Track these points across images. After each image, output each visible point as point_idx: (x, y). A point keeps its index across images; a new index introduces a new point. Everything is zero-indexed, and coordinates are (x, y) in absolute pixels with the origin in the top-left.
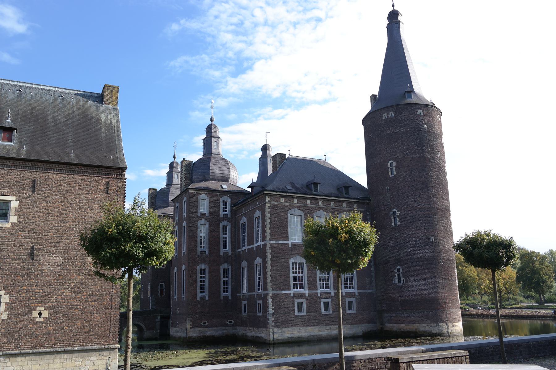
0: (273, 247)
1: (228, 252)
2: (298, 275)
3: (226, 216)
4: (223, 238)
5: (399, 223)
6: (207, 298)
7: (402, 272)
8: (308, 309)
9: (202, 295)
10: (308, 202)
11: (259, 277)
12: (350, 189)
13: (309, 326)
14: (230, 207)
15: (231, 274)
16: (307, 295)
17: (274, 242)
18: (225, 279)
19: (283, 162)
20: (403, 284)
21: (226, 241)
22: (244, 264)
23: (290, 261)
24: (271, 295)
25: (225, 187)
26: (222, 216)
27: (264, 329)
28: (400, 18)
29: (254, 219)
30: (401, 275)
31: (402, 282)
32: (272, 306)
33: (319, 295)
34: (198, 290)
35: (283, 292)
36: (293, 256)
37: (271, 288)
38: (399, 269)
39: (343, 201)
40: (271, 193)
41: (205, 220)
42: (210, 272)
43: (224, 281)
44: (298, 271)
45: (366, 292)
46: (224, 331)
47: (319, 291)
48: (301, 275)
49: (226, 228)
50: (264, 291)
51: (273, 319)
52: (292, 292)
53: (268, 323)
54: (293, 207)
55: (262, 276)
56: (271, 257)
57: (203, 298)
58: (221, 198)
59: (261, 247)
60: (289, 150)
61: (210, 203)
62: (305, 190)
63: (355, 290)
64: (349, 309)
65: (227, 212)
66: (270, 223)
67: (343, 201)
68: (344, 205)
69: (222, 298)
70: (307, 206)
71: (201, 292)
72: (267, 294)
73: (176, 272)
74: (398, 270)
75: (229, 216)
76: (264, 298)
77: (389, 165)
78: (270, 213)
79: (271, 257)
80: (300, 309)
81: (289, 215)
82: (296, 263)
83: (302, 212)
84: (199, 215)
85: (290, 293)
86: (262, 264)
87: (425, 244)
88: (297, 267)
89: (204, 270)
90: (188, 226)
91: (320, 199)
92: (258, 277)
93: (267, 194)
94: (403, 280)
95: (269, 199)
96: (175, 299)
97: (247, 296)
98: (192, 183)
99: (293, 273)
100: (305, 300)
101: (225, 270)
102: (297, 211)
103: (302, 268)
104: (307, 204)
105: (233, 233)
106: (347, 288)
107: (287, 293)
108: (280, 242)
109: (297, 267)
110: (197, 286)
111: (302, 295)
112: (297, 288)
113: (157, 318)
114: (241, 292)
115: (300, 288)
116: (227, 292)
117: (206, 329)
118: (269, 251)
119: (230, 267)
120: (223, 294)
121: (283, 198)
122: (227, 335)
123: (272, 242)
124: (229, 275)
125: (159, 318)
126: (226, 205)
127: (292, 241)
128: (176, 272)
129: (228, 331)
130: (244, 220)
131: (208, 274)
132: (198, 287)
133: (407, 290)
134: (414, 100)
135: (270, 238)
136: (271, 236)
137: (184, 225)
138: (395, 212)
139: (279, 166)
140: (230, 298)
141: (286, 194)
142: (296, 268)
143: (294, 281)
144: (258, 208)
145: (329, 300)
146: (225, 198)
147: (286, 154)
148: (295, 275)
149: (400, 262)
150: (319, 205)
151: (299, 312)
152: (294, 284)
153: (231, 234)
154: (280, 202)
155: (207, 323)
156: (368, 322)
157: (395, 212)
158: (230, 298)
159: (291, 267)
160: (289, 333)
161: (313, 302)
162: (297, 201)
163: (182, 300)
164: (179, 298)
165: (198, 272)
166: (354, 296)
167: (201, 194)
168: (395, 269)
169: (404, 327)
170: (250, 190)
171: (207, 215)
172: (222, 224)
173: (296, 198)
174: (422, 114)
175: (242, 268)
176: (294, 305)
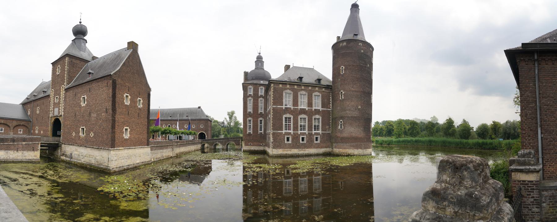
0: (274, 109)
1: (262, 113)
5: (343, 98)
6: (252, 133)
8: (292, 140)
10: (296, 87)
13: (293, 149)
16: (292, 134)
17: (275, 106)
18: (261, 125)
20: (343, 129)
24: (272, 133)
25: (262, 82)
26: (259, 95)
31: (342, 128)
33: (299, 134)
34: (248, 129)
36: (285, 113)
39: (316, 87)
41: (251, 97)
42: (253, 121)
44: (288, 121)
45: (326, 133)
47: (299, 132)
48: (289, 123)
52: (284, 131)
54: (287, 89)
57: (250, 133)
61: (253, 90)
63: (320, 132)
64: (316, 141)
66: (273, 97)
68: (317, 89)
69: (259, 133)
71: (249, 130)
74: (341, 122)
75: (263, 96)
78: (273, 92)
84: (248, 95)
87: (356, 109)
88: (288, 119)
89: (251, 120)
93: (272, 83)
100: (291, 136)
101: (261, 121)
102: (288, 91)
108: (278, 107)
109: (288, 119)
110: (247, 127)
111: (290, 134)
112: (287, 130)
116: (262, 131)
117: (251, 147)
120: (259, 132)
122: (261, 150)
123: (273, 106)
124: (263, 123)
129: (261, 148)
136: (273, 104)
138: (342, 92)
140: (263, 133)
142: (287, 120)
143: (285, 126)
145: (305, 136)
146: (262, 87)
148: (286, 123)
149: (342, 118)
156: (326, 147)
157: (342, 92)
158: (263, 133)
159: (284, 119)
160: (280, 152)
161: (296, 137)
166: (319, 135)
167: (249, 86)
171: (252, 95)
172: (260, 99)
176: (284, 138)
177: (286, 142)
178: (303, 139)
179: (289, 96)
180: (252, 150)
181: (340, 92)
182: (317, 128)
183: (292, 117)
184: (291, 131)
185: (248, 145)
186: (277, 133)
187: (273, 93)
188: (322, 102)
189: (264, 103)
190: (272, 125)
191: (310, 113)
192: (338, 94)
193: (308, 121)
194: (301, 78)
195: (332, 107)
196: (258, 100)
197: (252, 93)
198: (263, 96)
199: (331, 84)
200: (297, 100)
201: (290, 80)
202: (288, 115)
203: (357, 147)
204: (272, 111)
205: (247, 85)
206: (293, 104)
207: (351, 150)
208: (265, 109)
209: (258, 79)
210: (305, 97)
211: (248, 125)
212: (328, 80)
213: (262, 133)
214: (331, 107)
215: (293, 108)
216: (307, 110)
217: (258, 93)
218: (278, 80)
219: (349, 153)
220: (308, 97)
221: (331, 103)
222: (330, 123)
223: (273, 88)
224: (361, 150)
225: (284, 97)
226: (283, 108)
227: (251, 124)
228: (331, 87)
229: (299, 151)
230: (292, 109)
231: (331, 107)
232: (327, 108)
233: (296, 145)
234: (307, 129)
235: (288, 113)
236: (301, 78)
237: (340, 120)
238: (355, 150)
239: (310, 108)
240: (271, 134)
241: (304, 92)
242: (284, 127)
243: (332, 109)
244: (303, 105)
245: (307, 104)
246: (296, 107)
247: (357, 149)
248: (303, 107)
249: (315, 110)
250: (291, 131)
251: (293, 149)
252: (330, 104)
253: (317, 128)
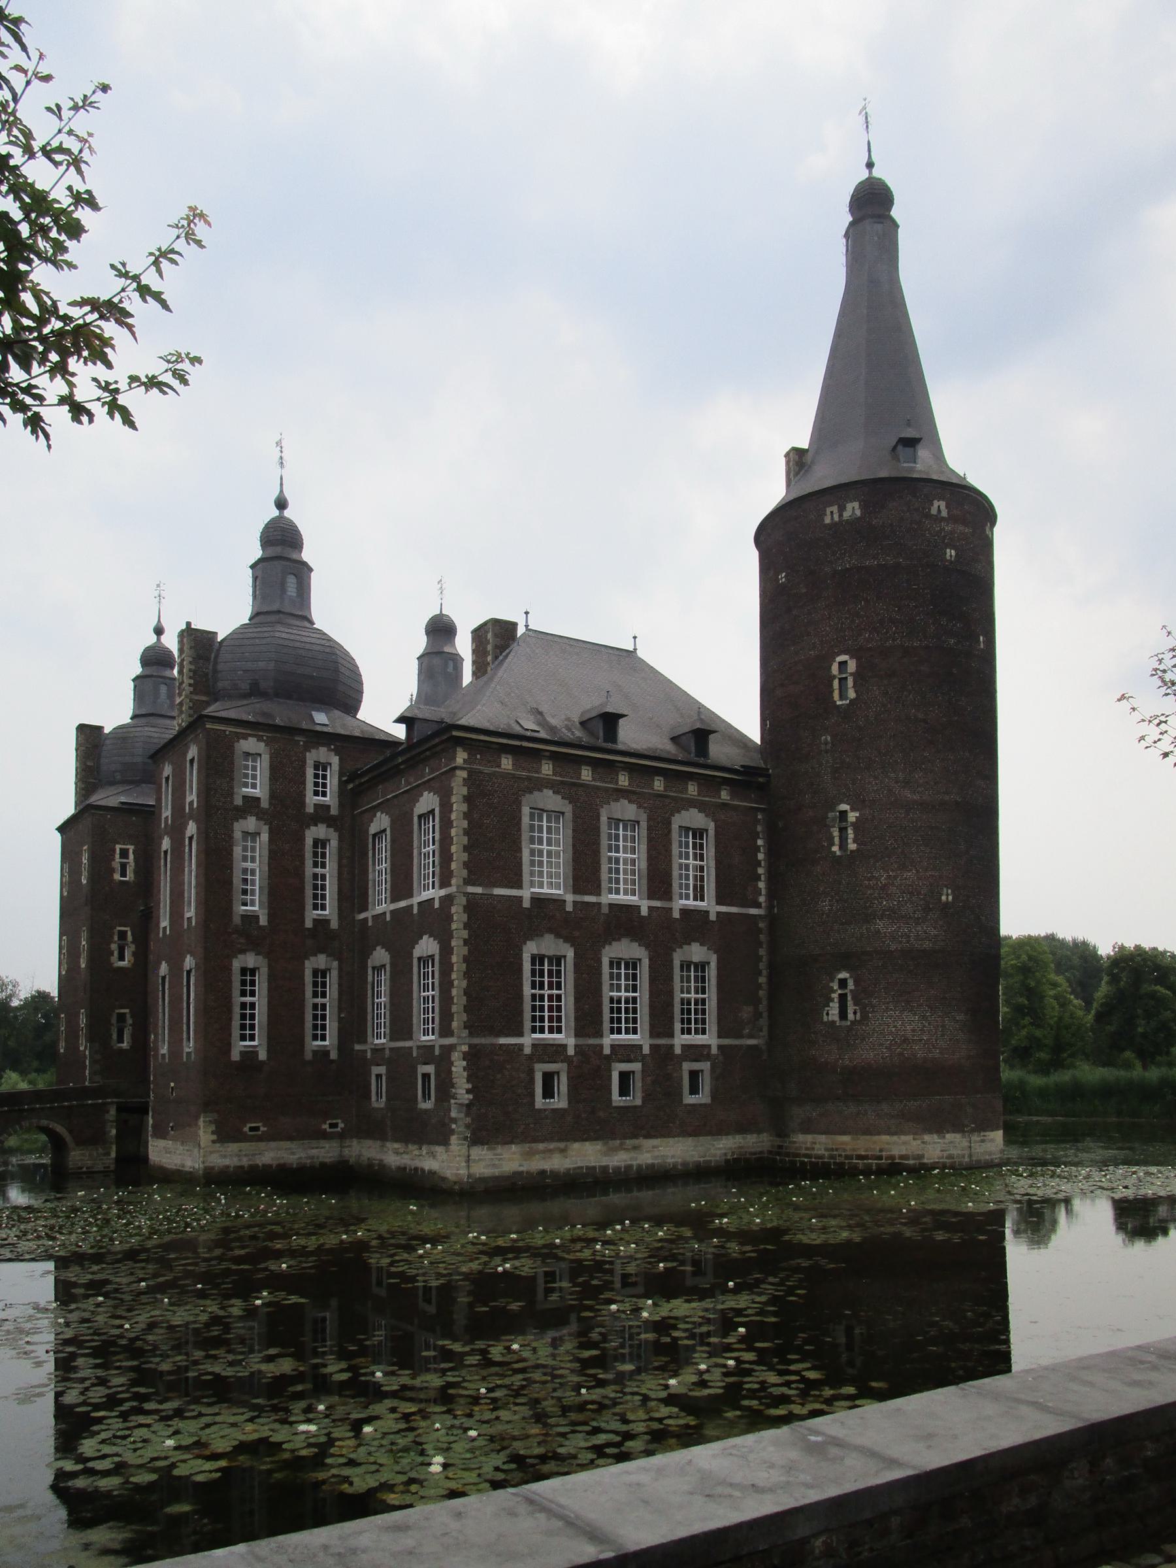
0: (472, 906)
2: (546, 992)
3: (322, 808)
4: (315, 876)
5: (852, 846)
6: (263, 1055)
7: (853, 987)
9: (245, 1046)
10: (586, 774)
11: (422, 994)
14: (336, 781)
15: (337, 986)
16: (571, 1052)
17: (479, 890)
18: (319, 1000)
19: (508, 646)
21: (323, 888)
22: (381, 956)
23: (525, 948)
24: (465, 1048)
25: (320, 718)
26: (310, 809)
27: (439, 1149)
29: (416, 819)
30: (849, 998)
31: (851, 1016)
32: (468, 1081)
33: (607, 1051)
34: (236, 1032)
35: (503, 1041)
36: (534, 933)
37: (465, 1028)
38: (845, 980)
40: (474, 736)
42: (272, 978)
43: (315, 1006)
47: (609, 1040)
49: (324, 847)
50: (442, 1035)
51: (468, 1120)
52: (528, 1040)
54: (539, 785)
55: (436, 993)
56: (466, 937)
57: (249, 1055)
58: (308, 754)
59: (437, 905)
60: (527, 613)
62: (578, 733)
65: (327, 799)
68: (692, 789)
69: (308, 1056)
70: (582, 785)
71: (243, 1038)
72: (451, 1048)
73: (164, 978)
74: (843, 983)
75: (334, 811)
76: (443, 1059)
78: (467, 799)
79: (466, 937)
80: (548, 1093)
82: (541, 958)
83: (567, 802)
85: (523, 1045)
86: (437, 958)
89: (253, 972)
90: (205, 834)
91: (622, 765)
92: (422, 994)
93: (460, 742)
94: (855, 1013)
95: (466, 757)
96: (163, 1055)
97: (387, 1052)
98: (216, 700)
99: (533, 987)
100: (565, 1065)
102: (550, 799)
103: (559, 972)
104: (583, 778)
105: (345, 861)
106: (689, 1033)
107: (512, 1045)
110: (230, 1019)
111: (555, 1052)
112: (542, 1031)
113: (108, 1112)
114: (369, 1039)
115: (551, 1031)
117: (262, 1145)
119: (335, 964)
121: (510, 757)
123: (471, 889)
125: (113, 1111)
126: (324, 777)
127: (533, 890)
128: (164, 978)
130: (381, 821)
131: (265, 985)
132: (236, 1023)
133: (864, 1039)
135: (464, 879)
136: (470, 872)
137: (188, 833)
139: (496, 658)
140: (334, 1055)
141: (517, 743)
144: (427, 785)
146: (322, 754)
147: (514, 625)
148: (537, 992)
149: (847, 959)
150: (617, 783)
151: (548, 1101)
152: (534, 1019)
153: (340, 866)
154: (499, 766)
155: (262, 1129)
158: (334, 1055)
159: (527, 966)
162: (551, 766)
163: (185, 1060)
164: (175, 1051)
165: (236, 978)
168: (833, 981)
170: (400, 732)
172: (313, 833)
173: (550, 758)
175: (374, 968)
176: (532, 1081)
179: (549, 828)
180: (267, 1167)
183: (570, 954)
184: (566, 1038)
185: (238, 1137)
187: (464, 807)
188: (717, 868)
193: (652, 980)
194: (610, 721)
195: (771, 896)
196: (302, 839)
198: (334, 811)
199: (757, 761)
200: (596, 853)
201: (552, 729)
202: (548, 945)
203: (938, 1123)
204: (458, 914)
205: (230, 729)
206: (576, 879)
207: (903, 1138)
209: (289, 697)
210: (633, 839)
213: (323, 1053)
214: (762, 899)
216: (644, 912)
217: (302, 795)
218: (492, 728)
219: (892, 1157)
220: (650, 840)
221: (761, 871)
223: (464, 774)
224: (958, 1136)
225: (525, 836)
226: (520, 899)
227: (253, 994)
228: (761, 780)
229: (606, 1154)
230: (569, 908)
231: (762, 899)
234: (647, 1027)
235: (550, 930)
236: (610, 721)
237: (839, 971)
238: (927, 1138)
239: (657, 904)
240: (455, 1056)
243: (770, 907)
245: (645, 881)
247: (940, 1130)
248: (622, 898)
249: (685, 912)
250: (566, 1038)
251: (576, 1145)
252: (758, 878)
253: (694, 1019)
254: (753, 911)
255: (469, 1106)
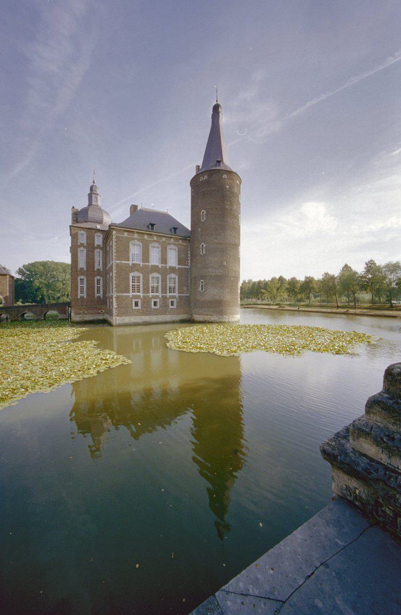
2: (136, 284)
5: (204, 252)
6: (85, 297)
10: (146, 237)
12: (177, 230)
16: (141, 297)
20: (205, 291)
25: (99, 227)
26: (96, 246)
28: (220, 110)
39: (171, 237)
46: (97, 317)
52: (131, 294)
53: (113, 314)
54: (134, 239)
57: (82, 297)
67: (171, 237)
68: (172, 240)
69: (96, 297)
74: (202, 282)
75: (101, 246)
77: (202, 213)
81: (130, 244)
84: (79, 244)
108: (123, 262)
110: (77, 290)
112: (135, 292)
118: (114, 268)
120: (96, 295)
123: (117, 261)
129: (101, 317)
134: (221, 167)
138: (203, 245)
140: (102, 297)
145: (158, 300)
146: (99, 234)
147: (137, 206)
148: (134, 284)
149: (203, 277)
153: (103, 258)
156: (184, 314)
158: (102, 297)
160: (127, 319)
161: (146, 301)
165: (79, 281)
169: (207, 318)
171: (85, 245)
174: (226, 178)
177: (134, 307)
178: (155, 304)
181: (201, 246)
182: (172, 290)
183: (142, 276)
184: (141, 294)
186: (122, 296)
189: (103, 256)
190: (114, 286)
191: (165, 272)
192: (198, 247)
196: (94, 252)
197: (85, 242)
198: (101, 246)
202: (136, 274)
208: (105, 264)
211: (79, 286)
212: (188, 230)
215: (143, 265)
216: (160, 267)
217: (94, 242)
222: (188, 283)
223: (115, 236)
230: (141, 266)
232: (185, 265)
233: (146, 311)
239: (163, 265)
240: (114, 297)
241: (156, 244)
242: (131, 288)
244: (155, 258)
246: (145, 264)
249: (170, 267)
250: (141, 294)
253: (172, 290)
254: (187, 267)
255: (116, 309)
